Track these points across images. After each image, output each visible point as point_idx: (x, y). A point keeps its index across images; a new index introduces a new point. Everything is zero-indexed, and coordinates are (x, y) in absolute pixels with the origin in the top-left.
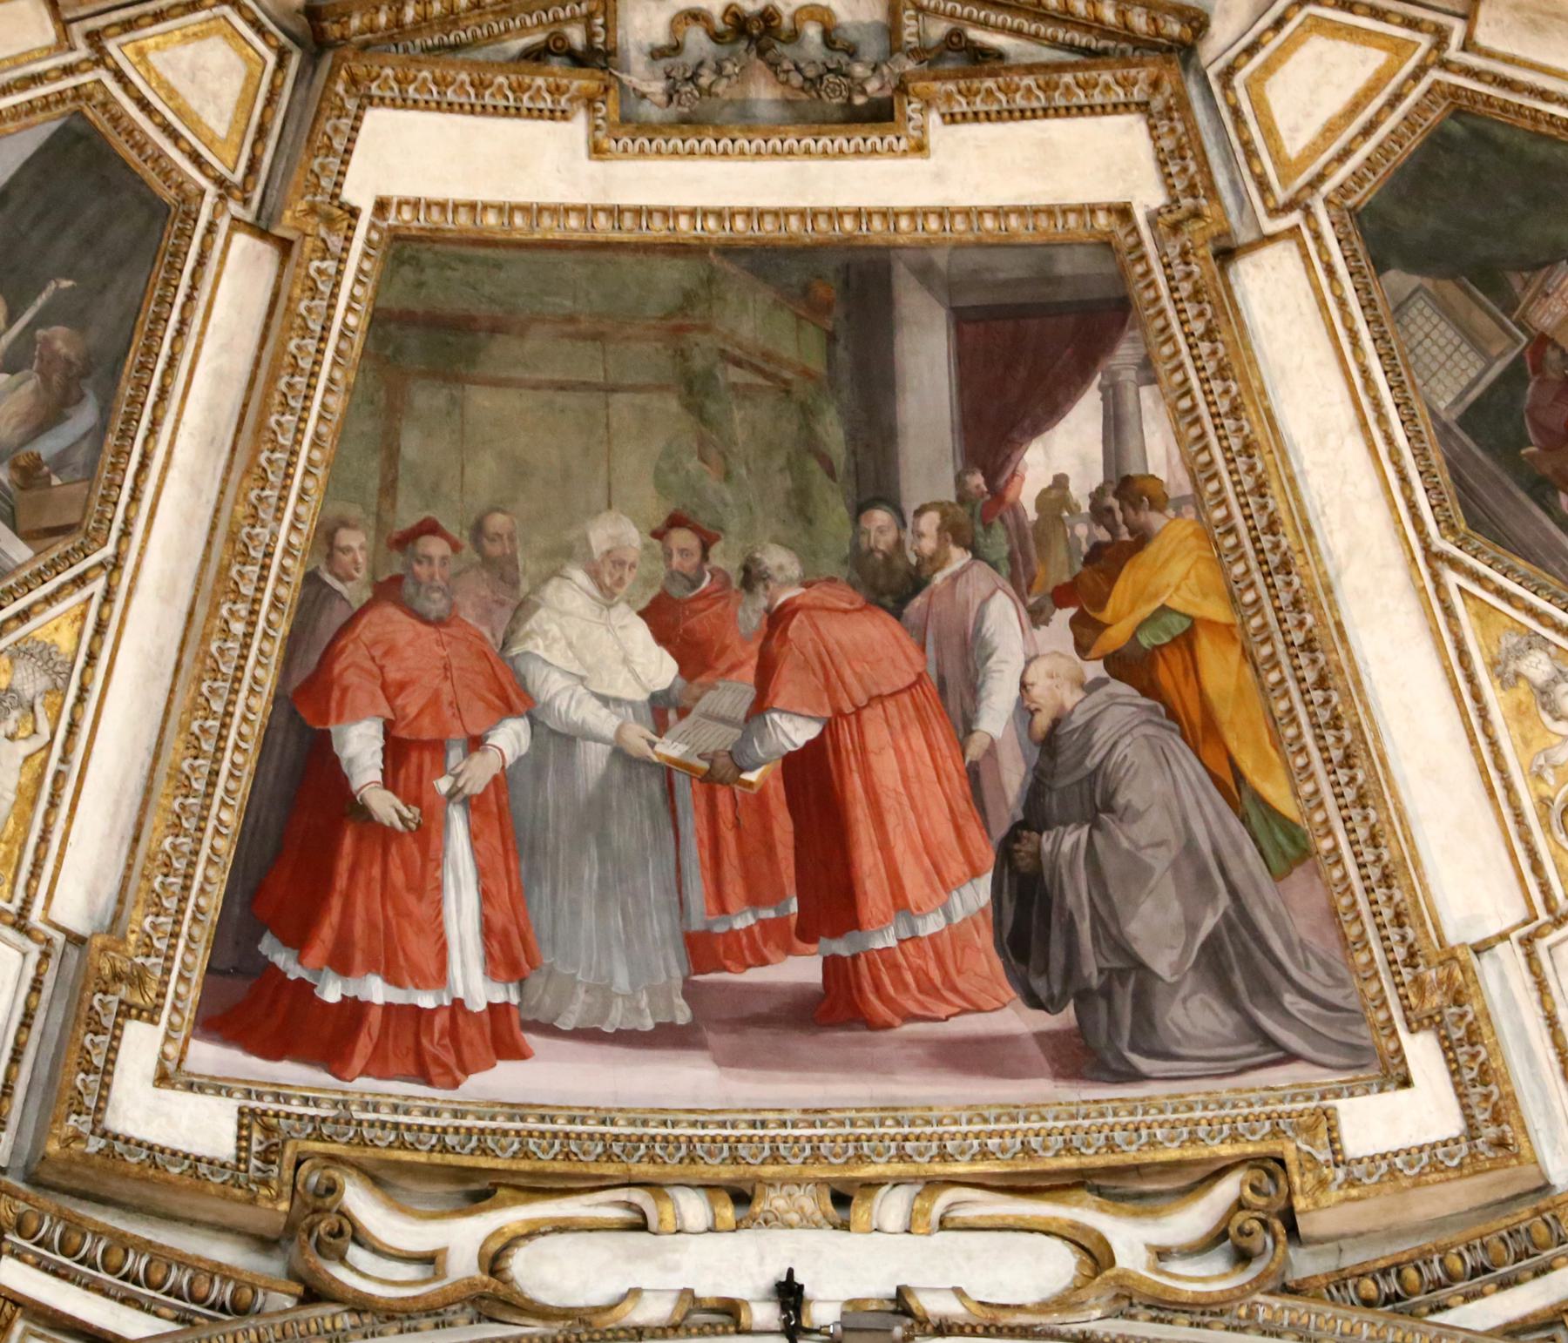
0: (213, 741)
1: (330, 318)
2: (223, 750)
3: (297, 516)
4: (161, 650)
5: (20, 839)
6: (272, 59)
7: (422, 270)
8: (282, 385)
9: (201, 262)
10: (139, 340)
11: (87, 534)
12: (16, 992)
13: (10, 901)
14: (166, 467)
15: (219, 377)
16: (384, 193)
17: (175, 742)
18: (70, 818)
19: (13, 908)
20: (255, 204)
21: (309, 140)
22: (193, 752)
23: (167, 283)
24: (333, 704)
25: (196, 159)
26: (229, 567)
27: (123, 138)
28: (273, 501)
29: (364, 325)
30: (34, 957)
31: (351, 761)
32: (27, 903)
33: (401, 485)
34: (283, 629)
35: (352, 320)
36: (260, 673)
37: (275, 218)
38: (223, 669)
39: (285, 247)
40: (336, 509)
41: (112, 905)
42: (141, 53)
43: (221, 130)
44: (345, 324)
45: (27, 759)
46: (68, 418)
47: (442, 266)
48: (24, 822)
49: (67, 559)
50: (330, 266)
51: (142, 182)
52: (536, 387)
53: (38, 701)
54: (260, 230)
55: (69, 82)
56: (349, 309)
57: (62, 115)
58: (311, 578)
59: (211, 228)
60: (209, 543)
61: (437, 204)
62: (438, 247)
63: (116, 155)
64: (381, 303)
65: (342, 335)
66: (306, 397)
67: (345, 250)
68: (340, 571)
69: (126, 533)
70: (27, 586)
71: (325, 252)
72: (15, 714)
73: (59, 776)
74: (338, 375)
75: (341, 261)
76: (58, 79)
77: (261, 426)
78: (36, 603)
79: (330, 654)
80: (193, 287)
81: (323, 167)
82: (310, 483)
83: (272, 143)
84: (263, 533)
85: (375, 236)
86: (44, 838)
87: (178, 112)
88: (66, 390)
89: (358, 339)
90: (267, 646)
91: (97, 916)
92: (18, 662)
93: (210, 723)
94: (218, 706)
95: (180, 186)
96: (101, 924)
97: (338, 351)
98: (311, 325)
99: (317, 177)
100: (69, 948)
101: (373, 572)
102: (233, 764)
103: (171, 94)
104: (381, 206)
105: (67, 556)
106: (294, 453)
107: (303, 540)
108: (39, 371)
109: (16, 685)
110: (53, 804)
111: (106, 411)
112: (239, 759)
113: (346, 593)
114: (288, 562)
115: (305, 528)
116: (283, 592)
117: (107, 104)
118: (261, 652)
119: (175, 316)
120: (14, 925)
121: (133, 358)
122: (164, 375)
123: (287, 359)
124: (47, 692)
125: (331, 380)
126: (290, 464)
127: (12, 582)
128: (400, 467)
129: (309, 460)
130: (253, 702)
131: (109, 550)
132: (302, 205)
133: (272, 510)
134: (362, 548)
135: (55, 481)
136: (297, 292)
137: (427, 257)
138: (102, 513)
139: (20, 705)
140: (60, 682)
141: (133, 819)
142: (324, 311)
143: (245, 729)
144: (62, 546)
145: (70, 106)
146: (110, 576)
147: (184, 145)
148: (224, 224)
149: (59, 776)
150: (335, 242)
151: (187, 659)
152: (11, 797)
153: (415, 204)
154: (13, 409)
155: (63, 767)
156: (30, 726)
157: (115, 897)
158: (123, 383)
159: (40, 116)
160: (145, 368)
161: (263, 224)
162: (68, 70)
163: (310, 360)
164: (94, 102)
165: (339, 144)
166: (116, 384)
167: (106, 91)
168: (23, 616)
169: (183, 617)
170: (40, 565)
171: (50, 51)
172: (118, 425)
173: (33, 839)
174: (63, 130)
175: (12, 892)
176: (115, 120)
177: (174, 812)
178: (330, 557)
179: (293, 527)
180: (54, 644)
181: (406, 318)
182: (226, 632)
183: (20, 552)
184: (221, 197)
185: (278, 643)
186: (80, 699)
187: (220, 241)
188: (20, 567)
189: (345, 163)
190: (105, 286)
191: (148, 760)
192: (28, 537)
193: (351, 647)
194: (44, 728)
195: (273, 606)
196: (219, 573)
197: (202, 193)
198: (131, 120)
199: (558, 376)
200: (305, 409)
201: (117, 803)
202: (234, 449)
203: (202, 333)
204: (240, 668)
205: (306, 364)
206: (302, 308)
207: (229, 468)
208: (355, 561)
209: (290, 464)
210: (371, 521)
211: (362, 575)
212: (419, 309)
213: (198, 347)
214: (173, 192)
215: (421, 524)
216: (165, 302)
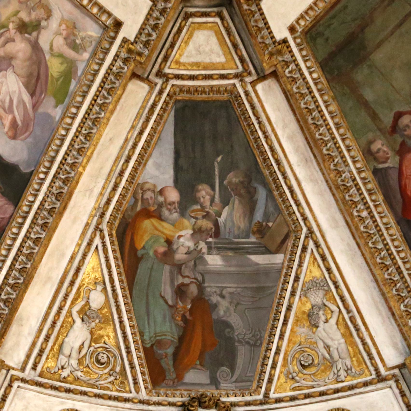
0: (389, 259)
1: (307, 83)
2: (394, 258)
3: (352, 157)
4: (348, 244)
5: (357, 351)
6: (218, 20)
7: (323, 35)
8: (310, 121)
9: (253, 107)
10: (257, 152)
11: (294, 231)
12: (398, 402)
13: (371, 375)
14: (299, 184)
15: (291, 138)
16: (289, 24)
17: (377, 272)
18: (367, 328)
19: (374, 376)
20: (253, 71)
21: (251, 34)
22: (385, 269)
23: (249, 125)
25: (223, 77)
26: (345, 198)
27: (196, 94)
28: (340, 161)
29: (321, 73)
30: (394, 385)
32: (377, 370)
33: (377, 112)
34: (380, 198)
35: (315, 75)
36: (385, 220)
37: (263, 70)
38: (371, 232)
39: (274, 74)
40: (364, 141)
41: (404, 344)
42: (178, 62)
43: (222, 59)
44: (313, 79)
45: (337, 324)
46: (257, 201)
47: (329, 26)
48: (354, 344)
49: (295, 246)
50: (292, 66)
51: (214, 101)
52: (392, 33)
53: (325, 301)
54: (262, 78)
55: (165, 95)
56: (311, 73)
57: (172, 107)
58: (376, 172)
59: (247, 94)
60: (334, 195)
61: (308, 9)
62: (321, 22)
63: (199, 101)
64: (320, 60)
65: (316, 84)
66: (322, 117)
67: (293, 56)
68: (381, 160)
69: (305, 219)
70: (290, 268)
71: (287, 64)
72: (321, 313)
73: (352, 319)
74: (326, 98)
75: (295, 61)
76: (160, 99)
77: (315, 141)
78: (297, 270)
79: (403, 190)
80: (258, 118)
81: (262, 38)
82: (348, 142)
83: (241, 47)
84: (346, 175)
85: (298, 41)
86: (364, 344)
87: (205, 69)
88: (249, 192)
89: (323, 79)
90: (380, 209)
91: (403, 352)
92: (308, 295)
93: (383, 254)
94: (380, 246)
95: (226, 90)
96: (406, 353)
97: (319, 90)
98: (303, 92)
99: (263, 43)
100: (403, 371)
101: (393, 149)
102: (402, 259)
103: (197, 65)
104: (292, 29)
105: (294, 245)
106: (334, 138)
107: (362, 162)
108: (236, 195)
109: (313, 303)
110: (358, 330)
111: (265, 185)
112: (402, 255)
113: (391, 165)
114: (363, 175)
115: (359, 158)
116: (369, 186)
117: (182, 89)
118: (379, 213)
119: (260, 134)
120: (379, 381)
121: (260, 160)
122: (273, 156)
123: (305, 111)
124: (326, 295)
125: (325, 102)
126: (335, 144)
127: (284, 271)
128: (373, 106)
129: (341, 135)
130: (391, 232)
131: (305, 230)
132: (266, 57)
133: (343, 165)
134: (383, 145)
135: (270, 224)
136: (289, 86)
137: (321, 29)
138: (293, 220)
139: (320, 308)
140: (326, 288)
141: (387, 309)
142: (303, 83)
143: (396, 243)
144: (290, 243)
145: (171, 102)
146: (312, 238)
147: (215, 77)
148: (249, 88)
149: (352, 319)
150: (287, 57)
151: (358, 240)
152: (343, 341)
153: (302, 17)
154: (238, 215)
155: (350, 315)
156: (329, 312)
157: (403, 340)
158: (264, 171)
159: (165, 115)
160: (266, 159)
161: (262, 75)
162: (161, 92)
163: (313, 103)
164: (178, 93)
165: (261, 24)
166: (262, 174)
167: (178, 86)
168: (297, 279)
169: (346, 227)
170: (288, 256)
171: (150, 93)
172: (274, 186)
173: (361, 347)
174: (176, 111)
175: (369, 371)
176: (188, 92)
177: (396, 295)
178: (376, 159)
179: (354, 162)
180: (314, 277)
181: (332, 56)
182: (362, 219)
183: (279, 258)
184: (241, 80)
185: (383, 204)
186: (337, 287)
187: (253, 95)
188: (283, 263)
189: (268, 28)
190: (232, 147)
191: (375, 285)
192: (277, 251)
193: (407, 181)
194: (334, 308)
195: (370, 194)
196: (343, 203)
197: (234, 85)
198: (193, 86)
199: (397, 22)
200: (325, 120)
201: (377, 308)
202: (315, 156)
203: (273, 130)
204: (377, 226)
205: (312, 106)
206: (295, 90)
207: (319, 164)
208: (384, 152)
209: (335, 144)
210: (378, 133)
211: (391, 154)
212: (334, 48)
213: (276, 135)
214: (226, 95)
215: (394, 117)
216: (254, 132)
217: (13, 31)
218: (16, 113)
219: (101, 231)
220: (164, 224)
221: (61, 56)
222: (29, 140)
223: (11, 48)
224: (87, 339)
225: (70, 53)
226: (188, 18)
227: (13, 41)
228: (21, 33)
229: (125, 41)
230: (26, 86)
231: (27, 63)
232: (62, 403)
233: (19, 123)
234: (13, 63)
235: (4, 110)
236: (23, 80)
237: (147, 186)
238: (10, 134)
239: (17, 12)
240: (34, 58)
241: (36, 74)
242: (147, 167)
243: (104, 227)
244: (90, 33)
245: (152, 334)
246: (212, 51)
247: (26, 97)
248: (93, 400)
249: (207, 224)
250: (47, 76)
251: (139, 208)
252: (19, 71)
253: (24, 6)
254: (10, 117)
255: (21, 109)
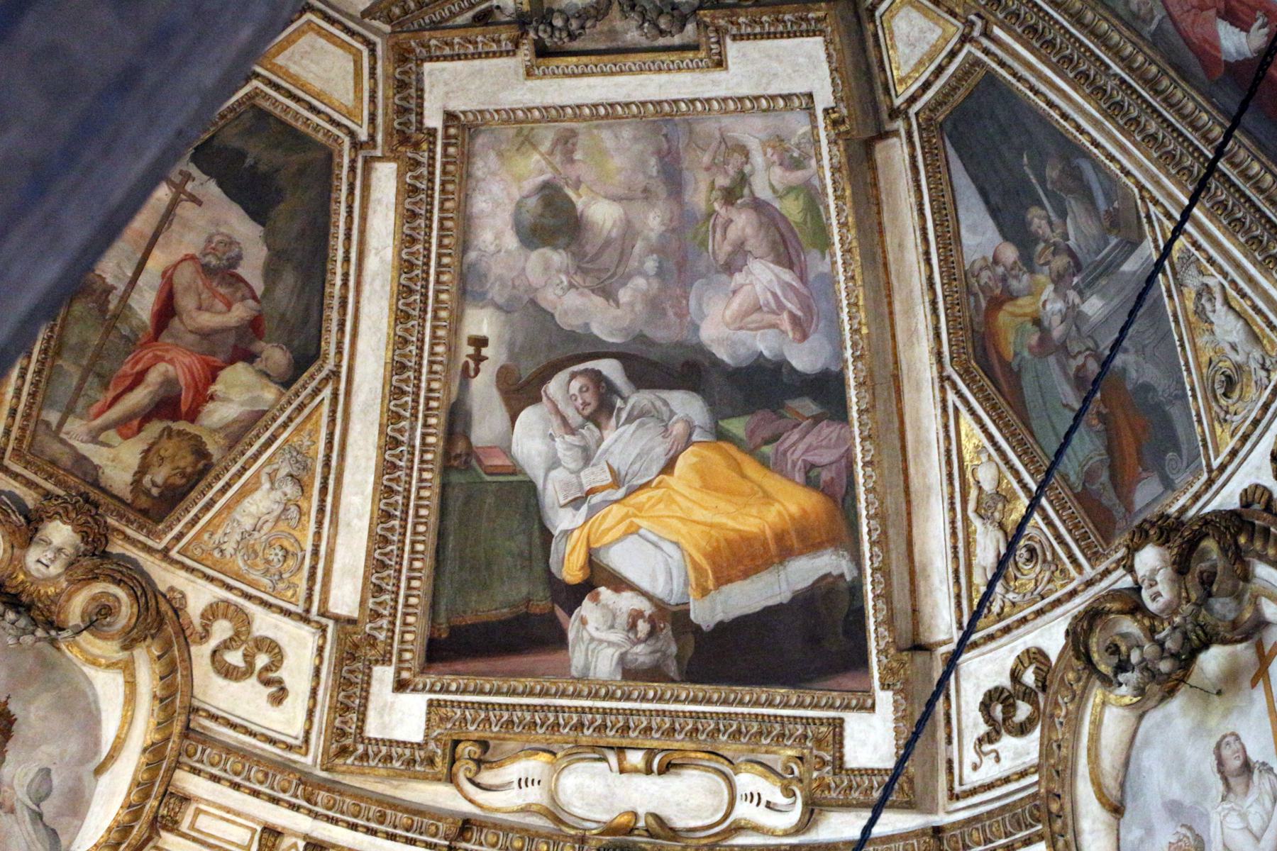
24: (1213, 52)
31: (1238, 52)
42: (902, 81)
59: (986, 51)
135: (1116, 205)
187: (993, 48)
198: (937, 93)
217: (723, 211)
218: (789, 305)
219: (949, 378)
220: (1020, 302)
221: (790, 189)
222: (821, 325)
223: (733, 233)
224: (998, 541)
225: (797, 176)
226: (873, 15)
227: (731, 221)
228: (732, 204)
229: (826, 111)
230: (778, 262)
231: (762, 233)
232: (1012, 651)
233: (799, 313)
234: (748, 248)
235: (773, 312)
236: (770, 258)
237: (977, 266)
238: (798, 336)
239: (713, 182)
240: (764, 219)
241: (778, 236)
242: (964, 241)
243: (949, 370)
244: (801, 131)
245: (1078, 469)
246: (921, 31)
247: (787, 276)
248: (1040, 621)
249: (1061, 262)
250: (792, 230)
251: (983, 304)
252: (759, 252)
253: (714, 170)
254: (785, 316)
255: (791, 295)
